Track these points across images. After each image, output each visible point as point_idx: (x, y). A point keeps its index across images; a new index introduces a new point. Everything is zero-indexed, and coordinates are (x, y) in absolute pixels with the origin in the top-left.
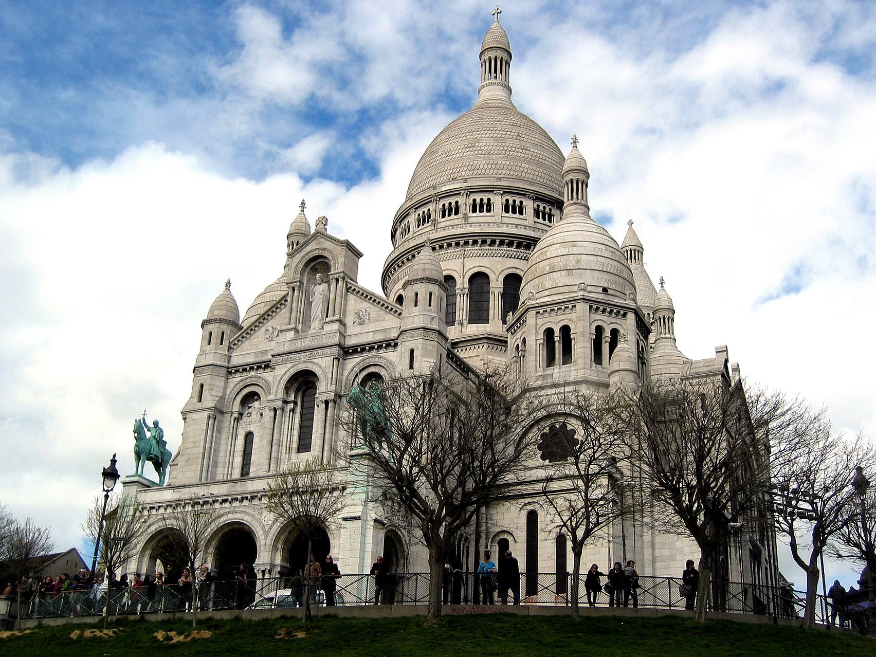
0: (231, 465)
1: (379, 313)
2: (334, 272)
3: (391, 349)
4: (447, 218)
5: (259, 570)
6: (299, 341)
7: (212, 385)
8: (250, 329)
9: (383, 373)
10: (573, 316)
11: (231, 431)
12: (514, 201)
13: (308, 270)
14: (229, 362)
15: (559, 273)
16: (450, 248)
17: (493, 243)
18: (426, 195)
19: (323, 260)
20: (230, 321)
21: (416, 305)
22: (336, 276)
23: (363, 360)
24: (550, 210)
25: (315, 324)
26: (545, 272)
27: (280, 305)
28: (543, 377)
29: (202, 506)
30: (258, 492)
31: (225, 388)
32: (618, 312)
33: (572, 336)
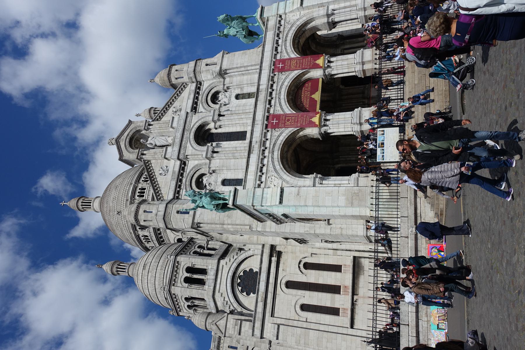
3: (202, 87)
6: (176, 140)
9: (213, 91)
19: (134, 140)
22: (147, 125)
23: (202, 103)
25: (170, 140)
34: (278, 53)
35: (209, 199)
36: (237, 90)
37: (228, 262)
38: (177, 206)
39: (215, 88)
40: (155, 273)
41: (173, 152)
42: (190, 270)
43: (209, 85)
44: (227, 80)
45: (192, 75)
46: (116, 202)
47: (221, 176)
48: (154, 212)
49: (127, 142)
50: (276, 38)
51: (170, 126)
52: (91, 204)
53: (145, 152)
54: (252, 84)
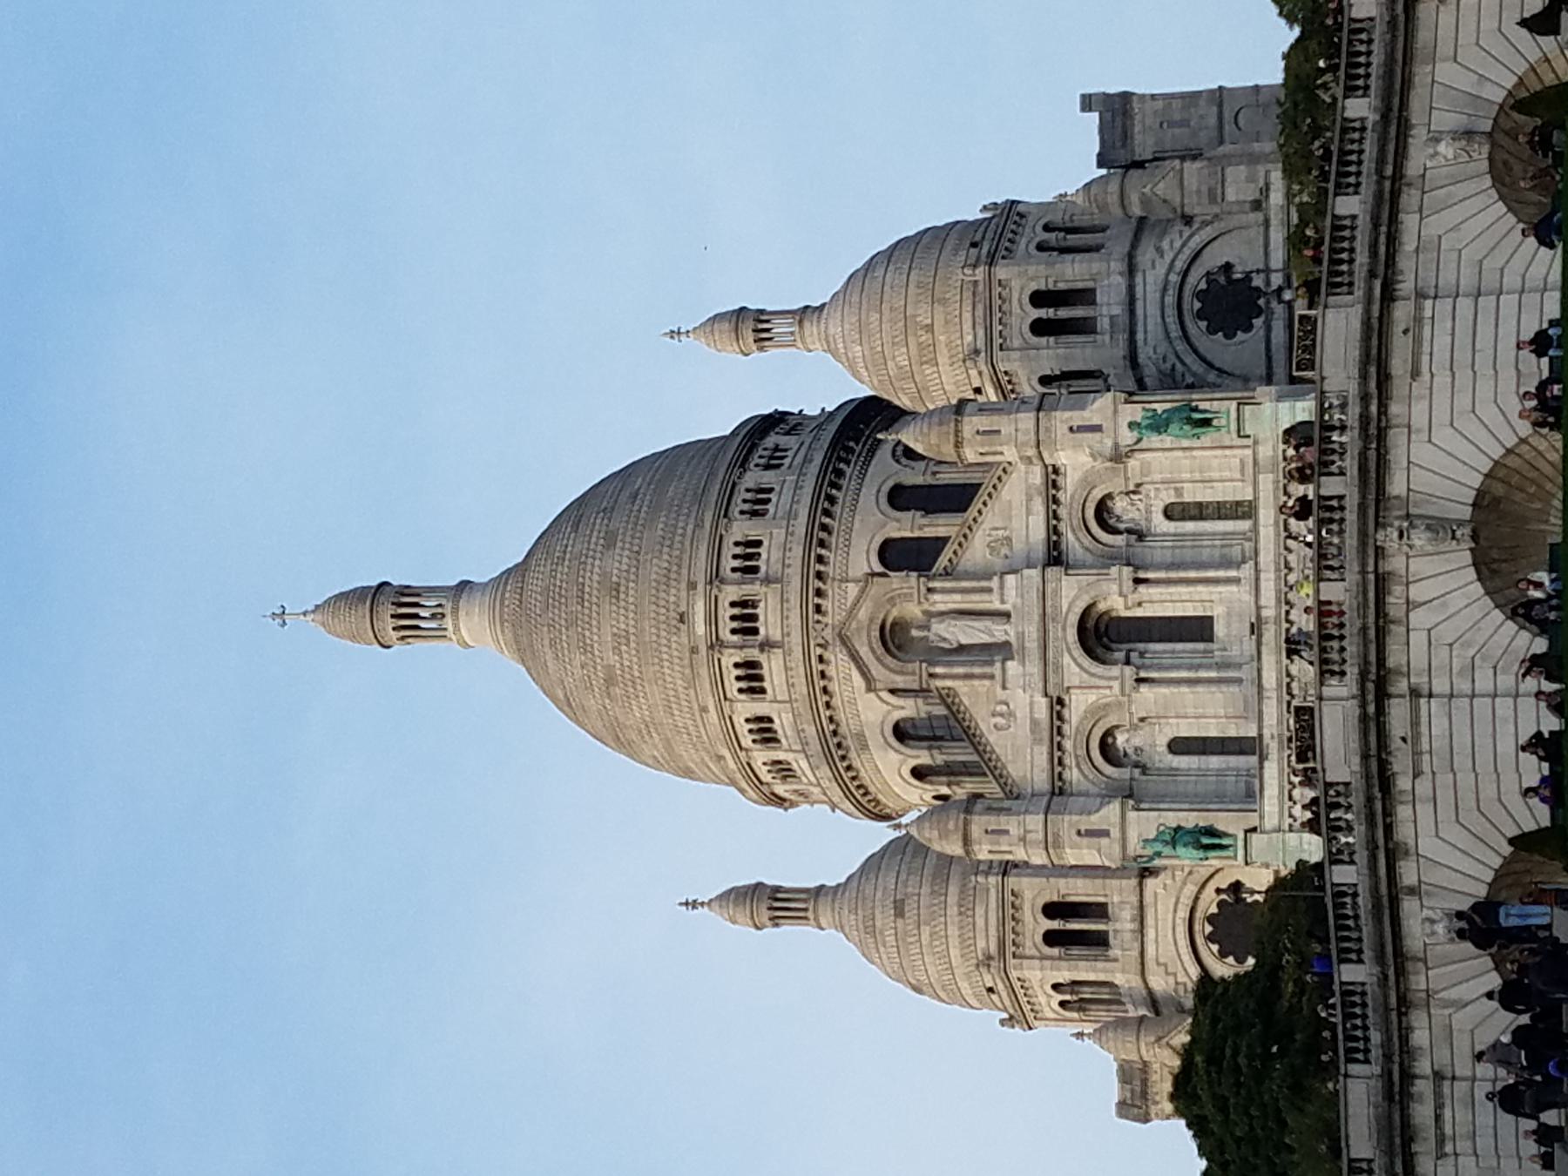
0: (1220, 773)
4: (760, 625)
6: (1027, 645)
9: (1098, 494)
10: (1016, 284)
11: (1163, 778)
12: (745, 501)
14: (1043, 795)
16: (823, 609)
17: (824, 527)
18: (704, 672)
22: (923, 589)
23: (1073, 531)
24: (765, 449)
25: (999, 632)
26: (931, 342)
28: (1112, 333)
31: (1086, 794)
32: (1015, 223)
33: (1051, 287)
35: (1195, 852)
37: (1169, 882)
38: (1075, 818)
40: (943, 926)
42: (1051, 910)
44: (1133, 463)
45: (1031, 452)
46: (634, 652)
48: (1014, 831)
49: (874, 640)
51: (995, 597)
53: (939, 670)
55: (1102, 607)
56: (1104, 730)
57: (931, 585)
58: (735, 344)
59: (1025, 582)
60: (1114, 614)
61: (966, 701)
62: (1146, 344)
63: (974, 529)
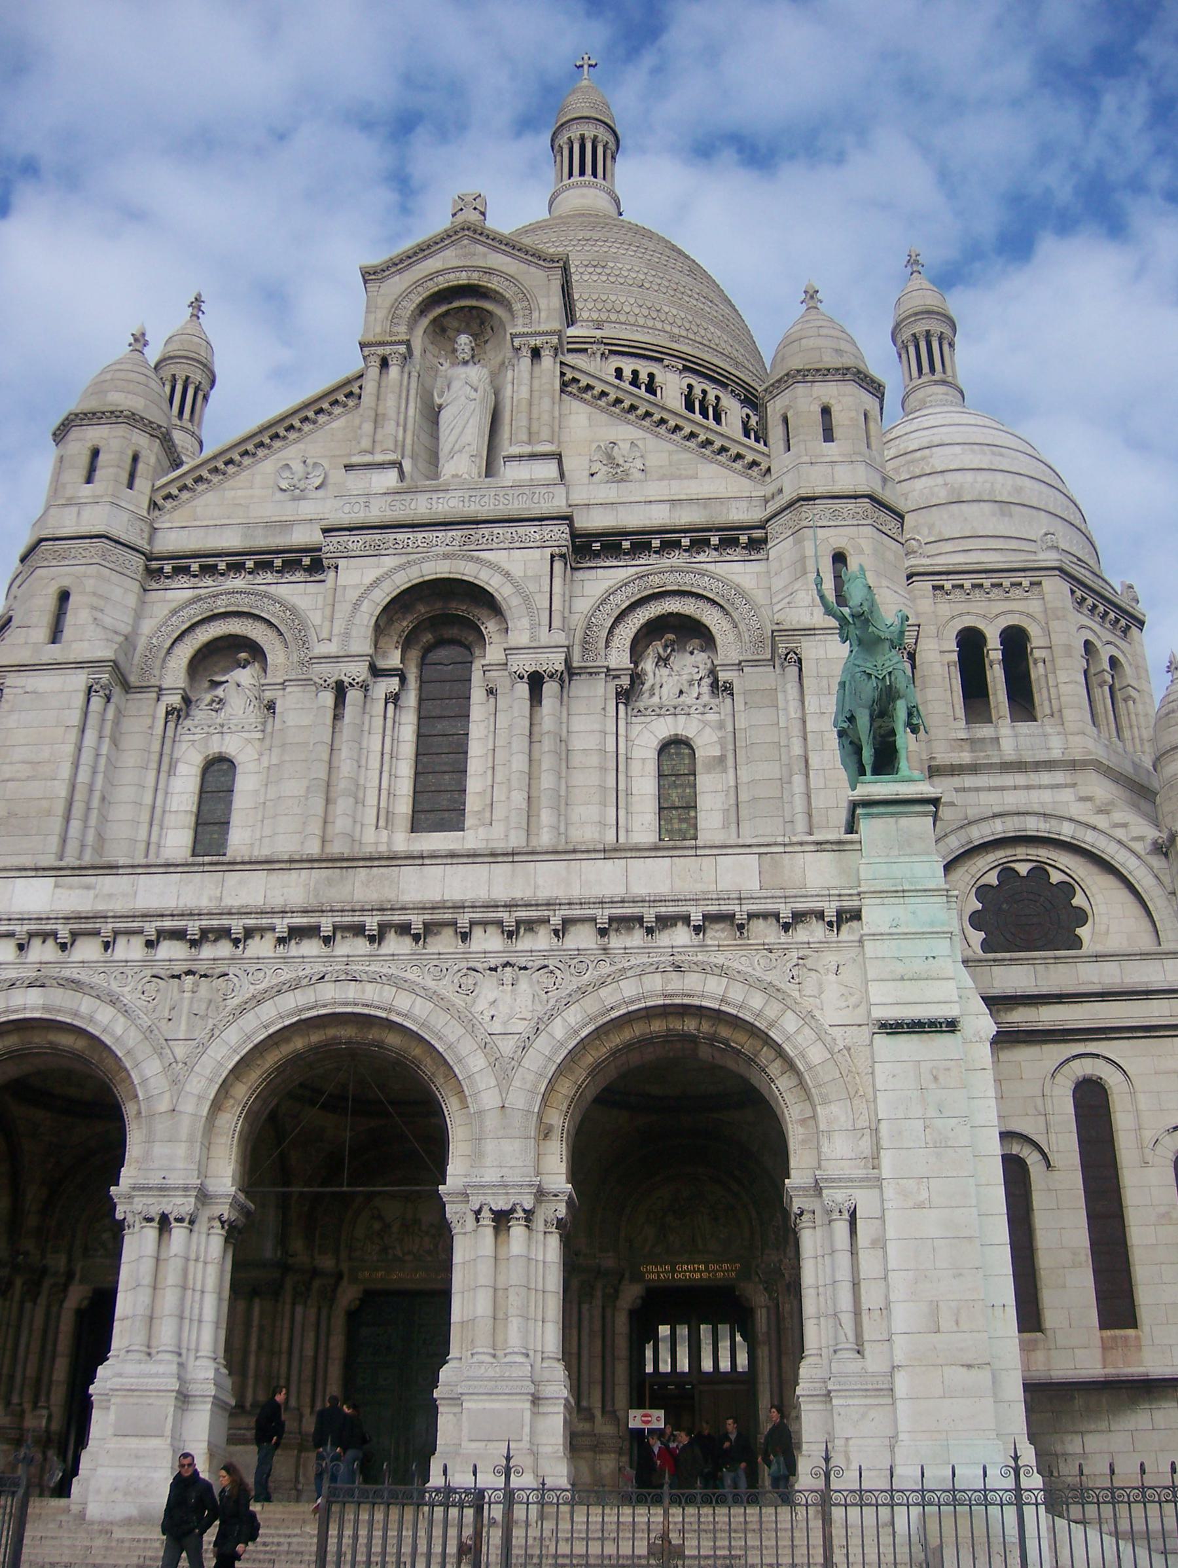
1: (675, 457)
2: (526, 330)
5: (478, 1212)
7: (101, 596)
8: (227, 457)
9: (710, 617)
10: (1034, 606)
11: (156, 747)
12: (704, 392)
13: (425, 322)
14: (151, 540)
15: (975, 506)
20: (160, 427)
21: (828, 435)
27: (331, 404)
28: (973, 743)
29: (194, 944)
30: (460, 907)
31: (138, 616)
33: (1037, 654)
34: (603, 932)
36: (715, 739)
39: (726, 625)
41: (362, 500)
43: (741, 592)
47: (249, 748)
49: (452, 276)
50: (696, 918)
51: (515, 450)
52: (576, 178)
54: (735, 813)
55: (490, 627)
56: (261, 640)
57: (542, 353)
58: (910, 312)
59: (543, 490)
60: (477, 652)
61: (335, 425)
62: (957, 790)
63: (646, 423)
